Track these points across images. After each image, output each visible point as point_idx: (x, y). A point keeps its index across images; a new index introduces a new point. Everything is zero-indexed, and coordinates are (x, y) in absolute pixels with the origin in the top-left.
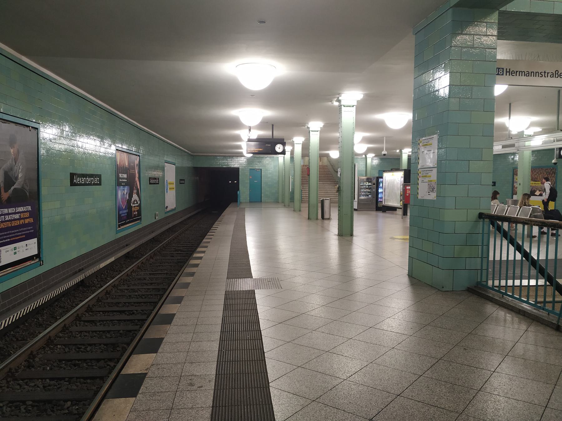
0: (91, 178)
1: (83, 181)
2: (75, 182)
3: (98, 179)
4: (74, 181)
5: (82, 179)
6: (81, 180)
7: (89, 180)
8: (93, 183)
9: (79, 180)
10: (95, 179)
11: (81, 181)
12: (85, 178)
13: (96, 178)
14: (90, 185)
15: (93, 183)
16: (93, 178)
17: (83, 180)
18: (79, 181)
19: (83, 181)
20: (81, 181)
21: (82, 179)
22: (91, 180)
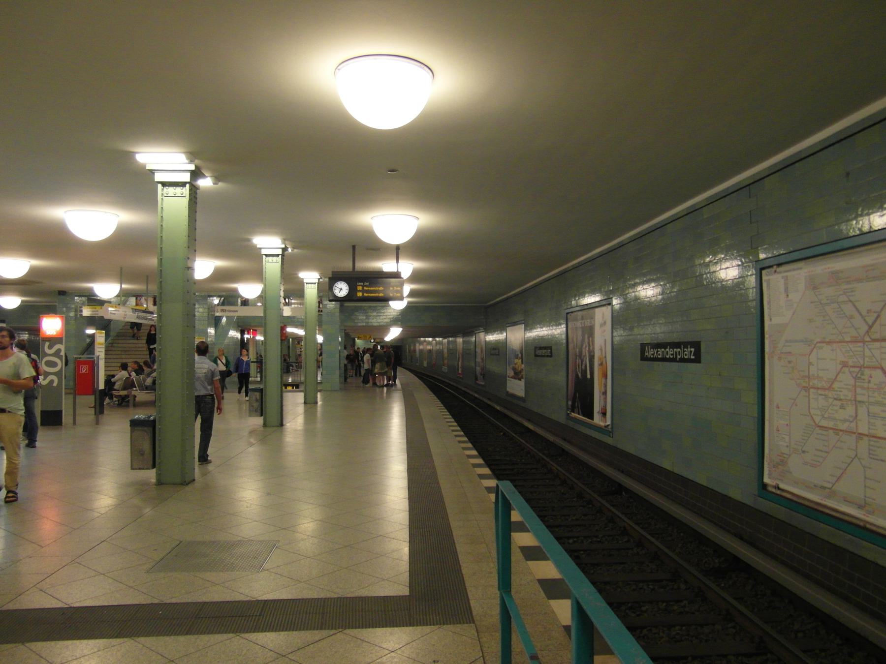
0: (675, 350)
1: (659, 355)
2: (647, 356)
3: (691, 352)
4: (646, 354)
5: (657, 352)
6: (655, 352)
7: (672, 353)
8: (679, 357)
9: (653, 353)
10: (684, 351)
11: (655, 354)
12: (663, 350)
13: (685, 349)
14: (673, 360)
15: (679, 357)
16: (679, 350)
17: (659, 353)
18: (652, 354)
19: (659, 355)
20: (655, 354)
21: (657, 352)
22: (676, 353)
